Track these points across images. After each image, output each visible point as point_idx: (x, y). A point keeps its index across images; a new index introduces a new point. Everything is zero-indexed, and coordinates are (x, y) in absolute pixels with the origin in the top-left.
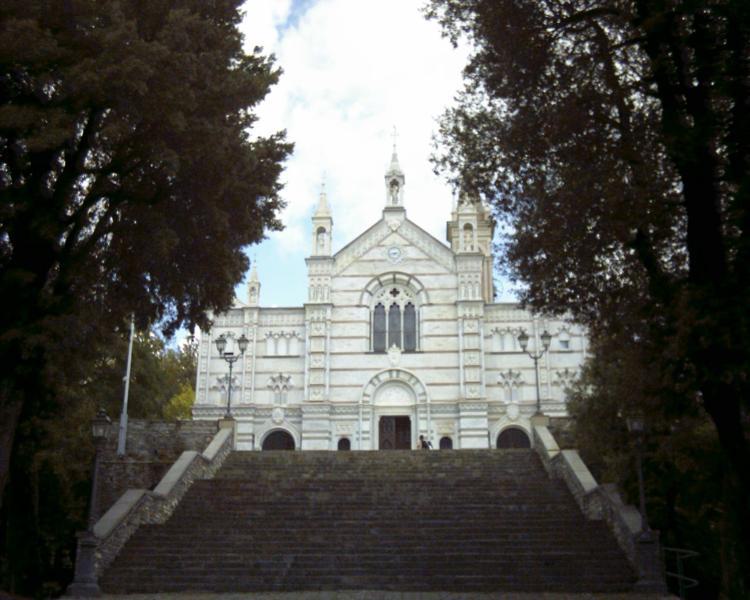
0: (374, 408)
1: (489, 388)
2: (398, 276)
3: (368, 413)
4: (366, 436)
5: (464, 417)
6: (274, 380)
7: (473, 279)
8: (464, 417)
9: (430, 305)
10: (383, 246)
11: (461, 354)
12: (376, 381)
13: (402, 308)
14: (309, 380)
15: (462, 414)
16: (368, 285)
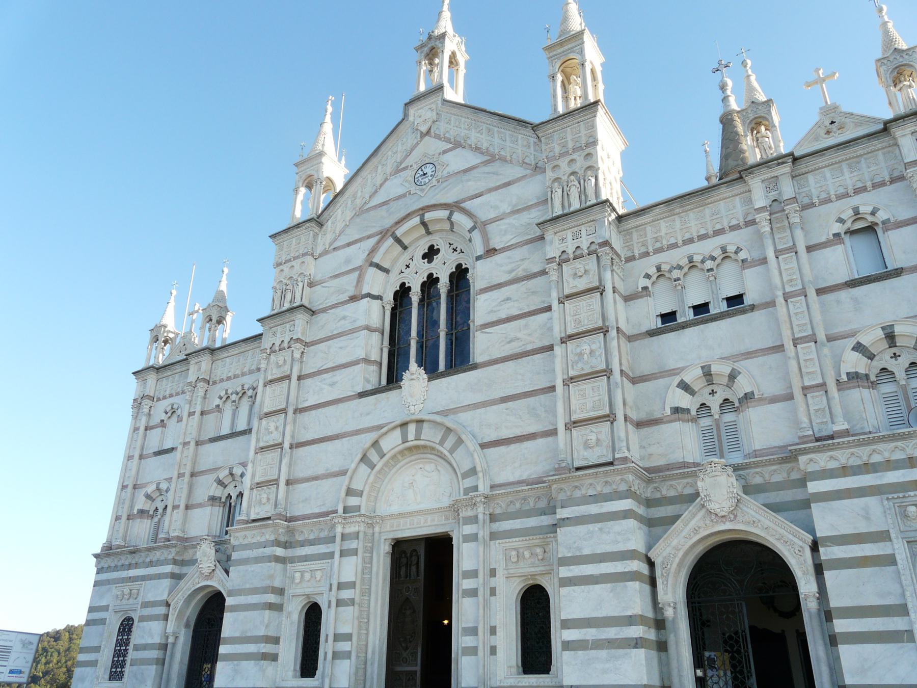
0: (372, 520)
1: (646, 431)
2: (428, 216)
3: (356, 535)
4: (346, 594)
5: (565, 522)
6: (220, 483)
8: (565, 522)
9: (491, 252)
11: (558, 350)
12: (373, 456)
13: (443, 286)
14: (253, 476)
15: (562, 513)
16: (373, 251)
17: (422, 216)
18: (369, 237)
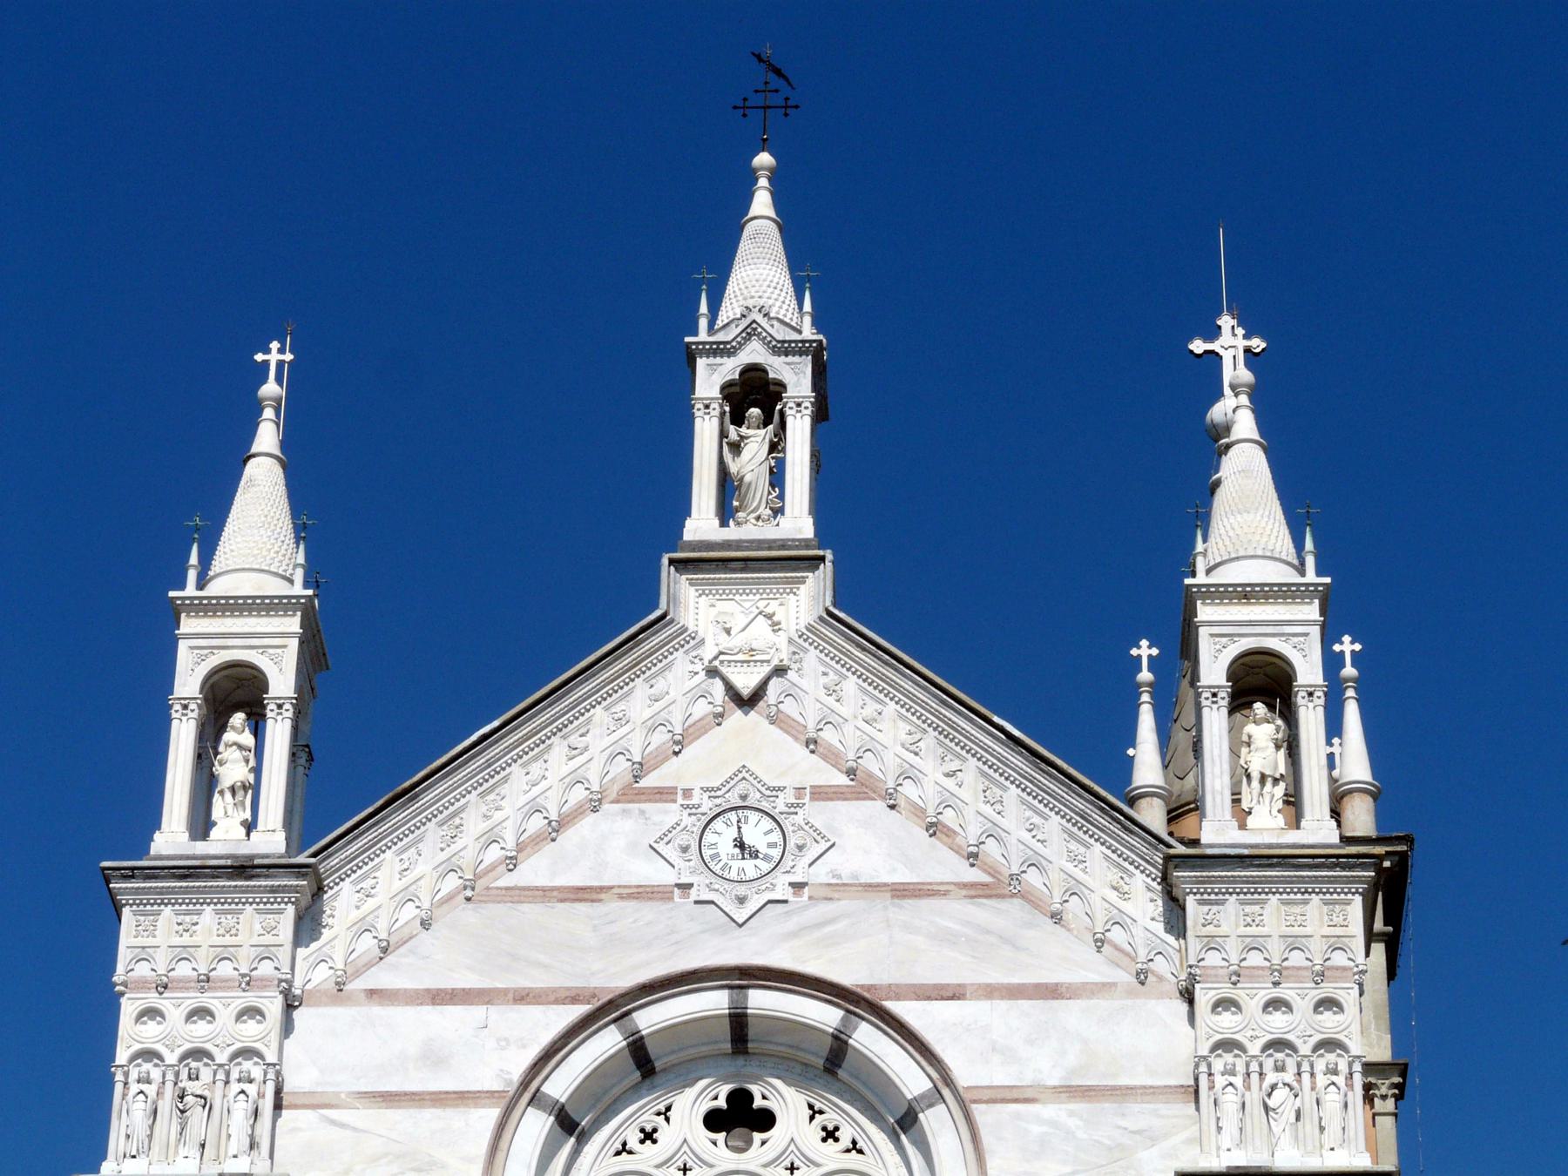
7: (1300, 1025)
10: (664, 794)
17: (934, 1097)
18: (523, 997)
